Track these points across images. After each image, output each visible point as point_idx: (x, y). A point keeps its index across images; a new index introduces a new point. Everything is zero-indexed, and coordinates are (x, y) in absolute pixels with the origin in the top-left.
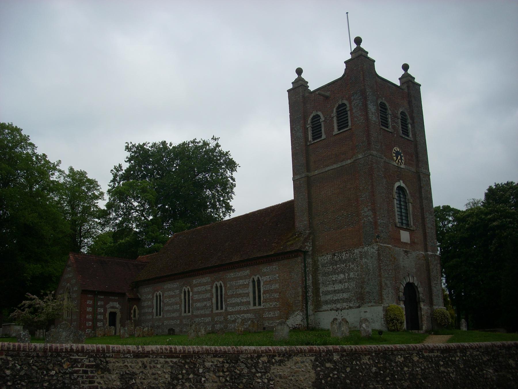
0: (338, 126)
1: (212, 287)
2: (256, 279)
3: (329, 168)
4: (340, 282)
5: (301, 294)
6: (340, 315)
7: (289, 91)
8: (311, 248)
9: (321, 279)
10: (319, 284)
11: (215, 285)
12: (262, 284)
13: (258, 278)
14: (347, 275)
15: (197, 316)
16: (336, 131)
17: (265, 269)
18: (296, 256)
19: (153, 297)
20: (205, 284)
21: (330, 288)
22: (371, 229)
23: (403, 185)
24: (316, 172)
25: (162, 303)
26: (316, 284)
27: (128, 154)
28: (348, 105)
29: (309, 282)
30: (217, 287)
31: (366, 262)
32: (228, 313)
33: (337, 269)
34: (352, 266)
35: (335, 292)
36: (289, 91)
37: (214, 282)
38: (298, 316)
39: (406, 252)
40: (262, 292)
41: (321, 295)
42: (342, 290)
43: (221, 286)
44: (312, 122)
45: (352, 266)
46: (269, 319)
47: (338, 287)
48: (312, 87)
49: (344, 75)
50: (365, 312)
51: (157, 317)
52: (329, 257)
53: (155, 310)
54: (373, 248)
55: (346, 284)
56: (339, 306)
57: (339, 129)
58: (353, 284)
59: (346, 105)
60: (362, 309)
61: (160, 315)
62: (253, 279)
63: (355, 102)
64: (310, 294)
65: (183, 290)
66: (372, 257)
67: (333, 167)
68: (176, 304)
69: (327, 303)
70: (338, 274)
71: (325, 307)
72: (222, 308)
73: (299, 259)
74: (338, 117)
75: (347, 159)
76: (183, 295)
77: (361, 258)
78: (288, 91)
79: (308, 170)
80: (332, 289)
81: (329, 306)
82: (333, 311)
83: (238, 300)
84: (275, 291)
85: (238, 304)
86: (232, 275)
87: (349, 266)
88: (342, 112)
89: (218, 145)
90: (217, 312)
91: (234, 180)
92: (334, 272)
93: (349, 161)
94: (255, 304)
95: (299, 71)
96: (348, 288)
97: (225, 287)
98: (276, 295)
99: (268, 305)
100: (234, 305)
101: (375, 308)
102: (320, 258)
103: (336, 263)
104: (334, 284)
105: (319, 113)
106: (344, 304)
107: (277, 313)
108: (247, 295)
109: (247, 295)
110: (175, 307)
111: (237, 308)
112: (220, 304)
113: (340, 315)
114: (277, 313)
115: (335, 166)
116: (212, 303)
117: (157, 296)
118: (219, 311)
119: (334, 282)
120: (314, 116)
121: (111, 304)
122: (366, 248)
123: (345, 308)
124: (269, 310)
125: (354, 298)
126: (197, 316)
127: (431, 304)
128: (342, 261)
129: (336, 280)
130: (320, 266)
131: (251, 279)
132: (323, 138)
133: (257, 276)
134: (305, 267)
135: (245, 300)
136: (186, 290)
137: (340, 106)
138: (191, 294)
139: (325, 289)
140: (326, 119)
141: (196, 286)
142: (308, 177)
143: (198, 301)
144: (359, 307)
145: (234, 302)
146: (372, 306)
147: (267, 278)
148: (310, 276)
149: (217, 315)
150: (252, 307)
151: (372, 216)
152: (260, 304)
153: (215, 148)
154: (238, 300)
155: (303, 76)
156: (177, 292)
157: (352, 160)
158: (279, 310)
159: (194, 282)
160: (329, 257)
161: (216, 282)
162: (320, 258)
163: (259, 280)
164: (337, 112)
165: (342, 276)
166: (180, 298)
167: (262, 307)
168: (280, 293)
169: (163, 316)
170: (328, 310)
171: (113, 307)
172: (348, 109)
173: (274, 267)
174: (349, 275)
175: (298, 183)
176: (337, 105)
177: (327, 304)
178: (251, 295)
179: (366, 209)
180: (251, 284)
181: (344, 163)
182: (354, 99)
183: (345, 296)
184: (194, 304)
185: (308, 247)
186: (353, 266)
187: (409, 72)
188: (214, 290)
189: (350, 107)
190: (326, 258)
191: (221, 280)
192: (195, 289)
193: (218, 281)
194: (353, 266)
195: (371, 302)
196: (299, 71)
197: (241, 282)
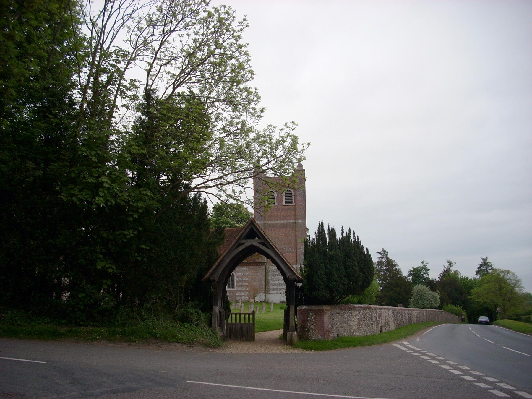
3: (277, 222)
9: (270, 277)
12: (235, 277)
18: (262, 265)
21: (276, 282)
24: (270, 222)
28: (293, 192)
40: (235, 281)
69: (274, 289)
71: (272, 292)
73: (264, 267)
81: (275, 291)
84: (246, 282)
93: (291, 221)
99: (240, 289)
102: (270, 267)
107: (247, 293)
114: (247, 293)
115: (282, 222)
124: (241, 291)
147: (238, 274)
152: (233, 287)
167: (235, 289)
172: (293, 194)
181: (288, 222)
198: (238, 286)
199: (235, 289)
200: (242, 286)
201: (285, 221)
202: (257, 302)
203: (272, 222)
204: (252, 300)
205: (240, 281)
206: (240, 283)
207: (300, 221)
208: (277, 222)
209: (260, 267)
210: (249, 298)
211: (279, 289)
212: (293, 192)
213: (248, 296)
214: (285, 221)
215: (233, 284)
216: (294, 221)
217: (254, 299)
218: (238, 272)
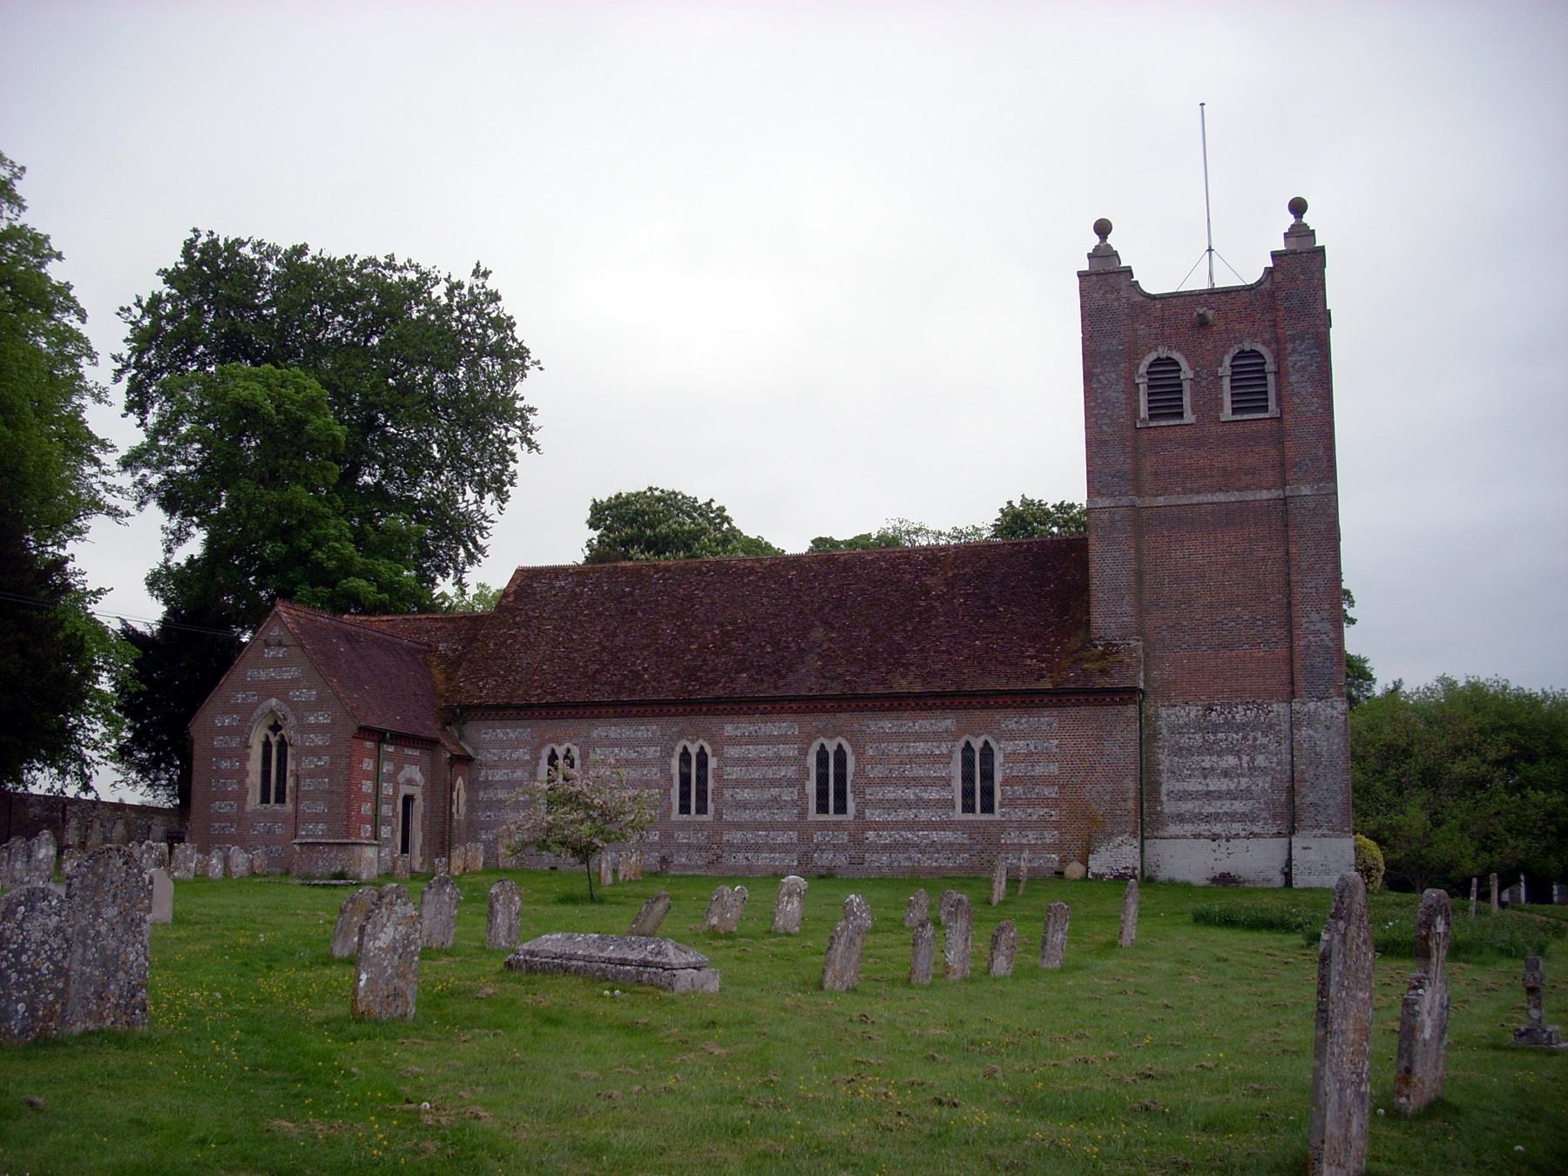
1: (804, 752)
2: (977, 745)
6: (1223, 849)
9: (1165, 761)
10: (1160, 772)
11: (815, 747)
12: (999, 759)
14: (1245, 759)
17: (1012, 722)
18: (1124, 702)
20: (770, 740)
21: (1194, 785)
22: (1328, 664)
24: (1161, 501)
28: (1269, 358)
37: (811, 738)
38: (1126, 849)
40: (998, 777)
41: (1164, 798)
42: (1229, 792)
43: (840, 753)
47: (1215, 784)
49: (1260, 282)
52: (1194, 711)
55: (1244, 781)
56: (1217, 828)
57: (1235, 411)
58: (1263, 783)
63: (1295, 358)
65: (679, 749)
66: (1328, 728)
67: (1215, 499)
71: (1173, 829)
73: (1131, 710)
75: (1261, 488)
76: (675, 763)
78: (1081, 275)
80: (1200, 788)
81: (1189, 828)
83: (910, 794)
84: (1047, 781)
86: (887, 725)
87: (1255, 739)
88: (1248, 372)
92: (1207, 749)
93: (1265, 495)
94: (968, 807)
96: (1248, 789)
97: (859, 755)
98: (1051, 792)
99: (1018, 815)
101: (1334, 840)
102: (1163, 712)
103: (1215, 729)
104: (1205, 777)
105: (1176, 356)
107: (1050, 837)
108: (946, 782)
109: (946, 782)
111: (903, 815)
113: (1223, 849)
114: (1050, 837)
115: (1220, 497)
116: (803, 794)
119: (1206, 773)
120: (1159, 359)
122: (1312, 706)
123: (1237, 836)
124: (1022, 826)
128: (1230, 725)
130: (1164, 731)
131: (961, 744)
133: (982, 739)
135: (934, 796)
138: (712, 763)
139: (1179, 786)
140: (1197, 374)
141: (735, 741)
143: (738, 784)
145: (891, 796)
147: (1010, 747)
151: (1332, 635)
152: (988, 807)
154: (910, 794)
156: (652, 752)
158: (1056, 828)
159: (729, 730)
160: (1194, 711)
161: (822, 740)
162: (1163, 712)
163: (987, 751)
165: (1231, 760)
166: (666, 771)
167: (997, 816)
168: (1062, 787)
170: (1185, 837)
171: (410, 782)
172: (1270, 367)
173: (1046, 719)
174: (1253, 760)
176: (1235, 350)
177: (1182, 821)
178: (958, 784)
179: (1314, 616)
180: (958, 757)
181: (1249, 496)
182: (1294, 351)
183: (1238, 806)
184: (727, 793)
186: (1265, 740)
188: (812, 761)
191: (840, 734)
192: (733, 752)
194: (1265, 740)
196: (1103, 228)
197: (921, 747)
198: (1010, 803)
199: (997, 816)
200: (1030, 803)
201: (1234, 496)
202: (1098, 877)
203: (1174, 500)
204: (1074, 870)
205: (1018, 780)
206: (1019, 790)
207: (1305, 490)
208: (1196, 499)
209: (1112, 710)
210: (1064, 861)
211: (1207, 819)
212: (1269, 358)
213: (1057, 847)
214: (1234, 496)
215: (988, 792)
216: (1275, 493)
217: (1085, 862)
218: (1011, 736)
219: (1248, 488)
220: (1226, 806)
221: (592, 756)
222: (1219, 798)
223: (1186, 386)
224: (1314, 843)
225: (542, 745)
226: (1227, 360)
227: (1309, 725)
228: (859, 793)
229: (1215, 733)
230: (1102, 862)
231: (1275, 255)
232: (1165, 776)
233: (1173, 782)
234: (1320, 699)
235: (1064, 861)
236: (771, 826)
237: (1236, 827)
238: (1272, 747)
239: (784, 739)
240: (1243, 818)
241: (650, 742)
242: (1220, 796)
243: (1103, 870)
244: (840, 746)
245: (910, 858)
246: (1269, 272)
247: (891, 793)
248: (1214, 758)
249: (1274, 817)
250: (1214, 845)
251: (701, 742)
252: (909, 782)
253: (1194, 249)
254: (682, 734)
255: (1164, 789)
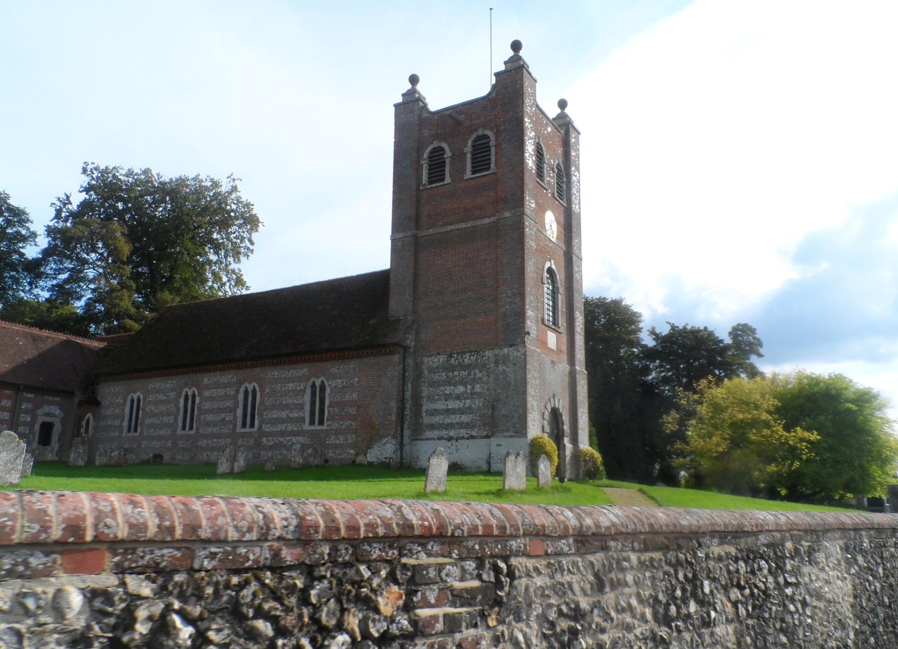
0: (473, 167)
1: (237, 391)
2: (318, 383)
4: (458, 397)
5: (394, 410)
6: (454, 447)
7: (397, 106)
8: (413, 343)
9: (425, 391)
10: (422, 398)
11: (243, 389)
12: (328, 391)
13: (323, 382)
14: (469, 387)
15: (206, 436)
16: (468, 175)
17: (335, 368)
18: (392, 353)
19: (125, 402)
21: (440, 405)
23: (554, 267)
24: (431, 231)
25: (141, 412)
26: (417, 398)
27: (85, 180)
28: (493, 138)
29: (408, 394)
30: (246, 392)
31: (504, 370)
32: (261, 433)
33: (453, 377)
34: (479, 375)
35: (448, 412)
36: (397, 106)
37: (241, 383)
38: (388, 446)
39: (553, 362)
40: (327, 403)
41: (424, 414)
42: (459, 409)
43: (254, 391)
44: (429, 157)
45: (479, 375)
46: (336, 446)
47: (453, 404)
48: (434, 105)
49: (490, 94)
50: (498, 445)
51: (129, 435)
53: (125, 424)
54: (518, 351)
55: (468, 402)
56: (452, 433)
57: (474, 172)
58: (478, 403)
59: (489, 137)
60: (494, 441)
61: (136, 431)
62: (314, 383)
64: (407, 412)
65: (184, 393)
66: (515, 364)
67: (459, 227)
68: (169, 415)
70: (455, 385)
71: (428, 434)
72: (252, 425)
73: (396, 358)
74: (473, 155)
75: (484, 217)
76: (182, 401)
77: (497, 363)
79: (417, 227)
80: (443, 407)
81: (436, 433)
82: (443, 441)
83: (284, 414)
85: (282, 421)
86: (274, 373)
87: (475, 374)
89: (234, 189)
90: (243, 430)
91: (252, 243)
92: (449, 382)
93: (487, 221)
94: (312, 422)
95: (414, 80)
96: (470, 408)
97: (262, 392)
99: (336, 425)
100: (275, 422)
102: (426, 360)
103: (453, 368)
105: (444, 145)
106: (462, 431)
109: (301, 407)
110: (165, 419)
111: (281, 427)
112: (249, 419)
113: (454, 447)
114: (351, 438)
116: (235, 417)
117: (132, 401)
118: (248, 430)
119: (447, 397)
120: (434, 148)
121: (47, 409)
122: (505, 350)
123: (463, 438)
124: (338, 432)
125: (479, 423)
126: (206, 436)
127: (575, 440)
129: (451, 394)
130: (426, 372)
131: (310, 383)
132: (446, 182)
133: (321, 379)
134: (404, 371)
135: (296, 415)
136: (190, 393)
137: (479, 138)
138: (197, 400)
139: (432, 406)
140: (453, 155)
141: (208, 387)
142: (416, 238)
143: (209, 411)
144: (487, 437)
145: (275, 416)
146: (511, 436)
148: (410, 385)
149: (243, 435)
150: (306, 427)
152: (321, 422)
153: (230, 193)
154: (284, 414)
155: (419, 87)
156: (172, 395)
157: (492, 219)
160: (442, 358)
161: (246, 384)
162: (426, 360)
163: (323, 388)
164: (473, 146)
165: (461, 389)
166: (177, 405)
167: (325, 427)
168: (359, 407)
169: (141, 433)
170: (434, 439)
171: (48, 415)
173: (353, 365)
174: (473, 388)
175: (399, 244)
176: (474, 136)
178: (307, 407)
180: (309, 391)
183: (465, 418)
184: (202, 417)
185: (410, 342)
186: (480, 375)
187: (567, 111)
188: (241, 396)
189: (496, 140)
190: (436, 360)
192: (207, 393)
193: (250, 383)
194: (480, 375)
195: (508, 431)
196: (414, 80)
197: (291, 386)
198: (332, 418)
199: (325, 427)
206: (336, 409)
207: (507, 214)
208: (449, 228)
210: (357, 454)
212: (493, 138)
219: (477, 218)
220: (456, 419)
221: (148, 399)
222: (454, 413)
223: (448, 161)
224: (503, 441)
225: (128, 394)
226: (470, 143)
227: (504, 363)
228: (261, 415)
229: (453, 372)
230: (374, 455)
231: (497, 75)
232: (425, 400)
233: (429, 404)
234: (511, 346)
235: (357, 454)
236: (219, 436)
237: (463, 432)
238: (484, 379)
239: (228, 385)
240: (466, 426)
241: (172, 390)
242: (452, 412)
243: (374, 460)
244: (254, 387)
245: (281, 454)
246: (494, 87)
247: (276, 414)
248: (452, 388)
249: (484, 425)
250: (449, 444)
251: (194, 389)
252: (284, 407)
253: (457, 82)
254: (186, 385)
255: (424, 408)
